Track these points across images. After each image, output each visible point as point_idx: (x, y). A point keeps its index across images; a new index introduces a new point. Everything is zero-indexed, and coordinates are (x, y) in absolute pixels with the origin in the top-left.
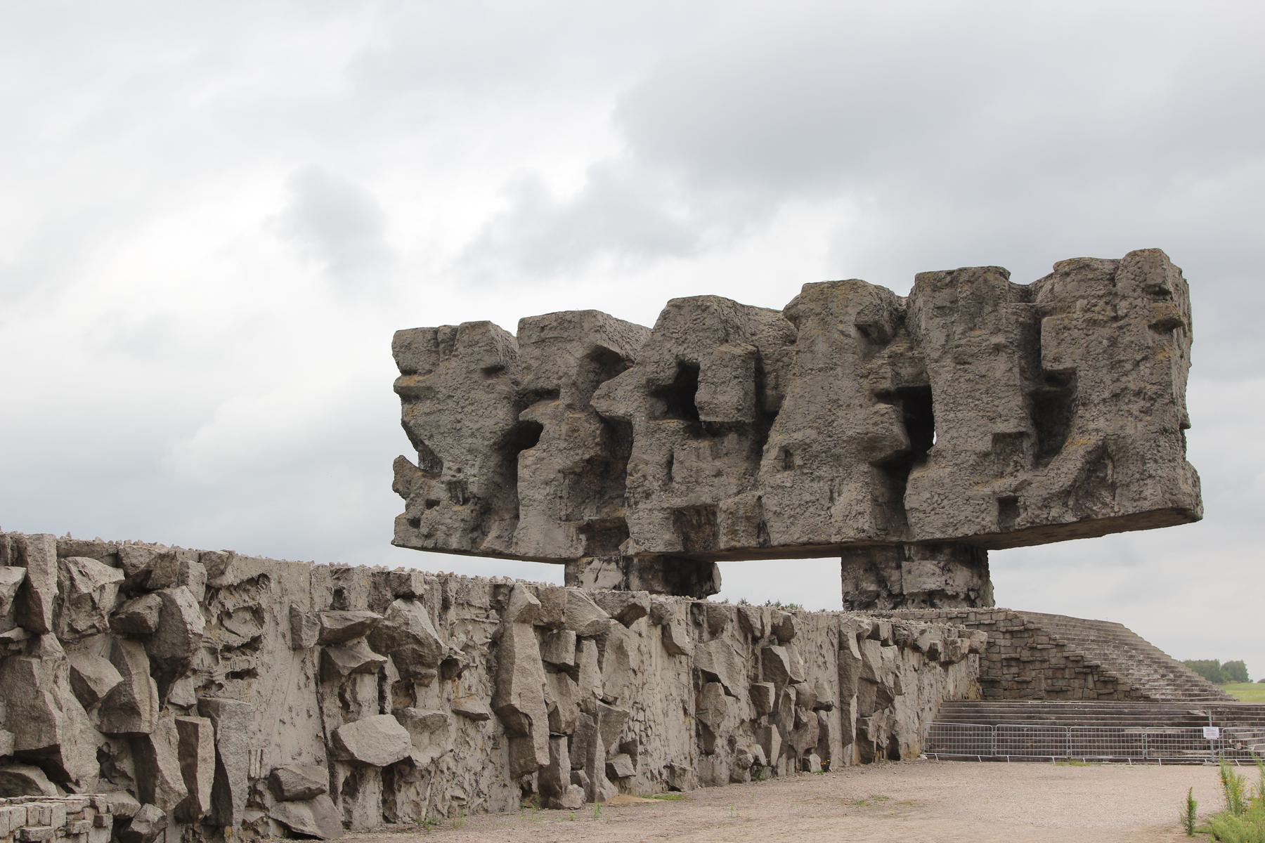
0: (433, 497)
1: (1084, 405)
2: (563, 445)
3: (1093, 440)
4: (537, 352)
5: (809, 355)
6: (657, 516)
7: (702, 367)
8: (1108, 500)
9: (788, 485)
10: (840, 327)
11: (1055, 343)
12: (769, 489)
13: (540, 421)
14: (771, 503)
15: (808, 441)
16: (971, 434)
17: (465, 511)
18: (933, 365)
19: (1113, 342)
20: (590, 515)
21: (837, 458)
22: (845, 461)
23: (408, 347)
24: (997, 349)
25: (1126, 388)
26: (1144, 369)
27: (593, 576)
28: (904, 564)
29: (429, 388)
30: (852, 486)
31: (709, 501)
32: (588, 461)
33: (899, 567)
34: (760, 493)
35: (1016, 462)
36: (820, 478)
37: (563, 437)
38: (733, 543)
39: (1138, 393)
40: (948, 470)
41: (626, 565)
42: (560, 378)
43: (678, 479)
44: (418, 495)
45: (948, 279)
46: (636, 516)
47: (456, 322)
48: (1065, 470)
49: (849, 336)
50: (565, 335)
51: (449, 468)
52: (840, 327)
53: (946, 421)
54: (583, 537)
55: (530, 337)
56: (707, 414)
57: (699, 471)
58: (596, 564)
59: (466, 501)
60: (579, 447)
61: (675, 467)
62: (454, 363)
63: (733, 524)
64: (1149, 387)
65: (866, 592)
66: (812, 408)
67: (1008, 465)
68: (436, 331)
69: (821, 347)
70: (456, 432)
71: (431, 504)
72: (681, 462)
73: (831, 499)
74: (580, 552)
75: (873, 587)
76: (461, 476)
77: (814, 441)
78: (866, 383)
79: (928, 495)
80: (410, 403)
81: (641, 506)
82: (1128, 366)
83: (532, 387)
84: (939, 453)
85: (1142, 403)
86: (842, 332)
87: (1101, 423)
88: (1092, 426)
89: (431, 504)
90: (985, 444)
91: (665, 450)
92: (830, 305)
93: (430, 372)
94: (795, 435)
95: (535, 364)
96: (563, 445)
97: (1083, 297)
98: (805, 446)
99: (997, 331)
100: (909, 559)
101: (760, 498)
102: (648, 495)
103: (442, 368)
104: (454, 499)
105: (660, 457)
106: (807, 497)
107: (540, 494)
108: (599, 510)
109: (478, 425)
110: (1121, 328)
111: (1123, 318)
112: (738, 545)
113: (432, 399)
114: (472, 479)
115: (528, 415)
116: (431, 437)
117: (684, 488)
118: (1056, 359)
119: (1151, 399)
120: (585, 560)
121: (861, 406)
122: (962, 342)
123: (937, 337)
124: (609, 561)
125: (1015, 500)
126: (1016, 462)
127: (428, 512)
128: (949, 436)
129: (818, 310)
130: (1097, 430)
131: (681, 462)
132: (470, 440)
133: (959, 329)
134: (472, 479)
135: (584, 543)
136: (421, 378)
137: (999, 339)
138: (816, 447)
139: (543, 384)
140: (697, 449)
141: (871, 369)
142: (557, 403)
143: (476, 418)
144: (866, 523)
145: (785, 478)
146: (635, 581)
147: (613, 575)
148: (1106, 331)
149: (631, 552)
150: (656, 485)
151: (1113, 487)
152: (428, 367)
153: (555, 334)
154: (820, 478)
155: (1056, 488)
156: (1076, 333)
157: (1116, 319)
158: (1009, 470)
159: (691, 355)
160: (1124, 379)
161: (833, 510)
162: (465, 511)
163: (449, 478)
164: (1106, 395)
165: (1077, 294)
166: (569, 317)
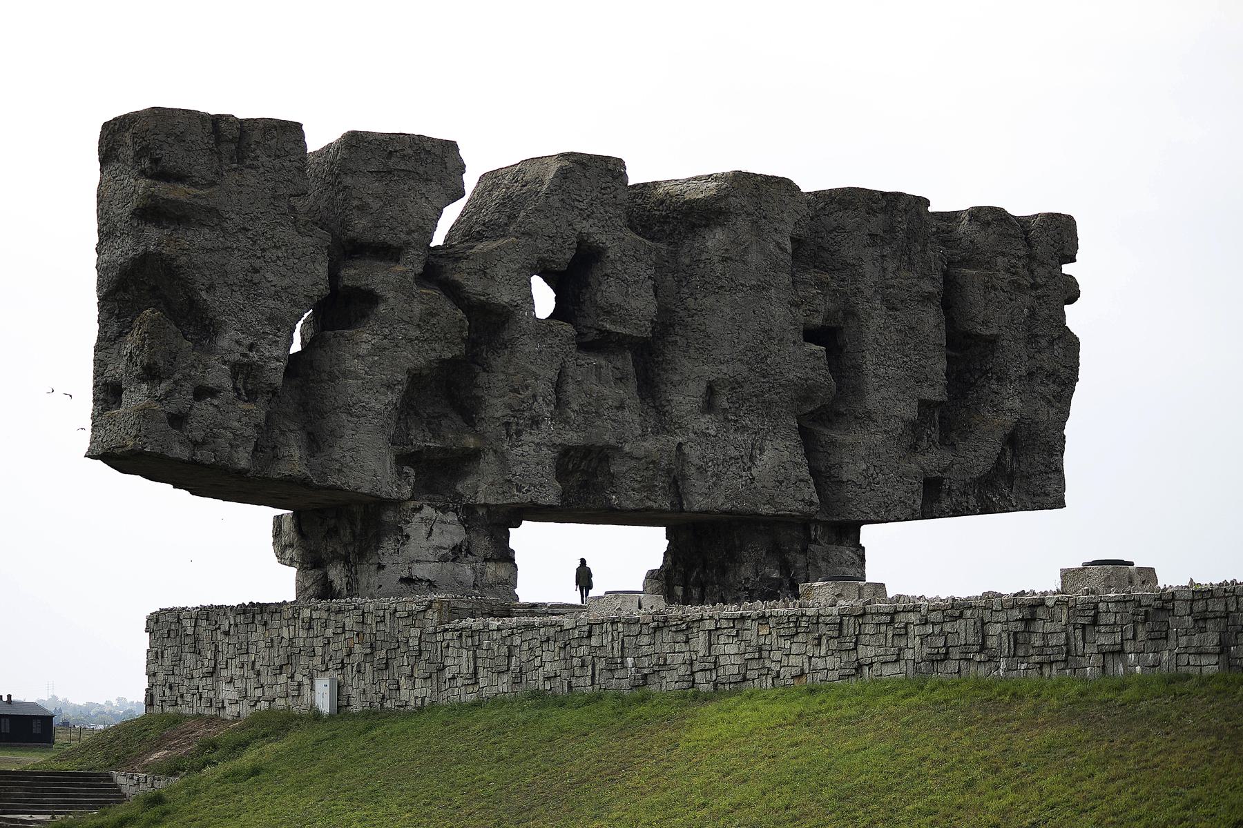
0: (211, 381)
1: (999, 379)
2: (413, 333)
3: (1009, 420)
4: (377, 187)
5: (741, 266)
6: (548, 454)
7: (610, 254)
8: (1006, 491)
9: (713, 433)
10: (776, 237)
11: (983, 303)
12: (692, 436)
13: (379, 290)
14: (694, 453)
15: (740, 379)
16: (900, 396)
17: (258, 410)
18: (866, 305)
19: (1033, 314)
20: (421, 439)
21: (769, 405)
22: (775, 410)
23: (180, 138)
24: (927, 298)
25: (1041, 368)
26: (1058, 349)
27: (424, 530)
28: (813, 547)
29: (211, 211)
30: (778, 443)
31: (613, 441)
32: (442, 362)
33: (804, 551)
34: (679, 440)
35: (929, 436)
36: (745, 428)
37: (416, 321)
38: (650, 503)
39: (1052, 375)
40: (879, 437)
41: (469, 514)
42: (409, 233)
43: (575, 406)
44: (187, 377)
45: (884, 203)
46: (515, 451)
47: (244, 110)
48: (983, 453)
49: (783, 250)
50: (421, 170)
51: (237, 342)
52: (776, 237)
53: (876, 376)
54: (406, 469)
55: (366, 162)
56: (614, 322)
57: (601, 398)
58: (428, 511)
59: (251, 396)
60: (438, 340)
61: (571, 388)
62: (250, 178)
63: (654, 477)
64: (1062, 370)
65: (770, 579)
66: (743, 336)
67: (920, 439)
68: (218, 119)
69: (755, 258)
70: (251, 285)
71: (202, 393)
72: (579, 383)
73: (752, 458)
74: (407, 491)
75: (776, 575)
76: (254, 356)
77: (746, 379)
78: (799, 313)
79: (864, 467)
80: (159, 225)
81: (525, 437)
82: (1044, 343)
83: (369, 237)
84: (869, 415)
85: (1052, 387)
86: (778, 244)
87: (1016, 403)
88: (1008, 405)
89: (202, 393)
90: (911, 412)
91: (556, 366)
92: (764, 205)
93: (212, 184)
94: (724, 368)
95: (376, 205)
96: (413, 333)
97: (1003, 254)
98: (735, 385)
99: (922, 276)
100: (815, 541)
101: (680, 444)
102: (535, 422)
103: (230, 180)
104: (235, 389)
105: (552, 374)
106: (732, 452)
107: (383, 402)
108: (436, 435)
109: (287, 282)
110: (1038, 298)
111: (1041, 286)
112: (655, 506)
113: (212, 229)
114: (274, 364)
115: (351, 275)
116: (210, 288)
117: (581, 419)
118: (985, 323)
119: (1064, 384)
120: (411, 505)
121: (794, 343)
122: (895, 282)
123: (870, 271)
124: (444, 510)
125: (939, 481)
126: (929, 436)
127: (196, 404)
128: (879, 396)
129: (751, 209)
130: (1011, 411)
131: (579, 383)
132: (271, 303)
133: (891, 266)
134: (274, 364)
135: (412, 479)
136: (194, 191)
137: (927, 286)
138: (748, 389)
139: (383, 236)
140: (598, 367)
141: (805, 297)
142: (400, 268)
143: (283, 270)
144: (810, 492)
145: (706, 423)
146: (483, 544)
147: (451, 533)
148: (1028, 300)
149: (481, 499)
150: (546, 411)
151: (1010, 478)
152: (210, 177)
153: (410, 166)
154: (745, 428)
155: (976, 473)
156: (1002, 296)
157: (1034, 286)
158: (925, 444)
159: (600, 238)
160: (1038, 356)
161: (754, 471)
162: (258, 410)
163: (237, 357)
164: (1023, 372)
165: (1000, 249)
166: (428, 145)
